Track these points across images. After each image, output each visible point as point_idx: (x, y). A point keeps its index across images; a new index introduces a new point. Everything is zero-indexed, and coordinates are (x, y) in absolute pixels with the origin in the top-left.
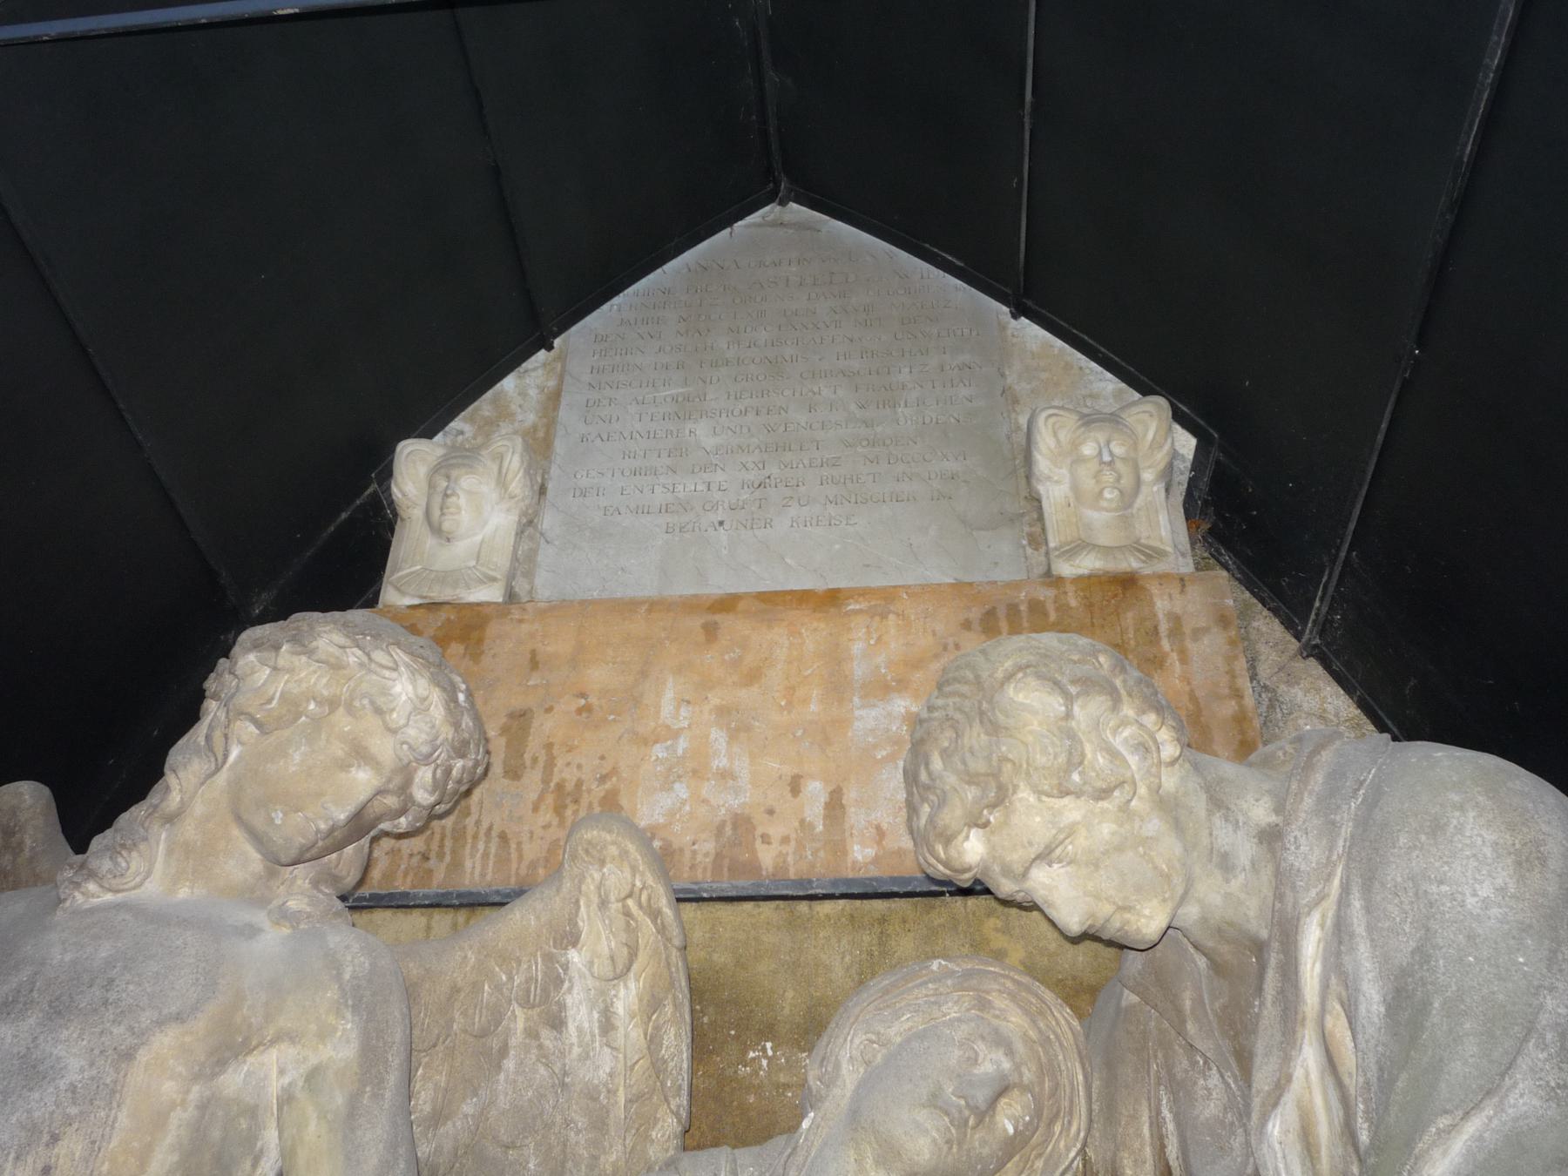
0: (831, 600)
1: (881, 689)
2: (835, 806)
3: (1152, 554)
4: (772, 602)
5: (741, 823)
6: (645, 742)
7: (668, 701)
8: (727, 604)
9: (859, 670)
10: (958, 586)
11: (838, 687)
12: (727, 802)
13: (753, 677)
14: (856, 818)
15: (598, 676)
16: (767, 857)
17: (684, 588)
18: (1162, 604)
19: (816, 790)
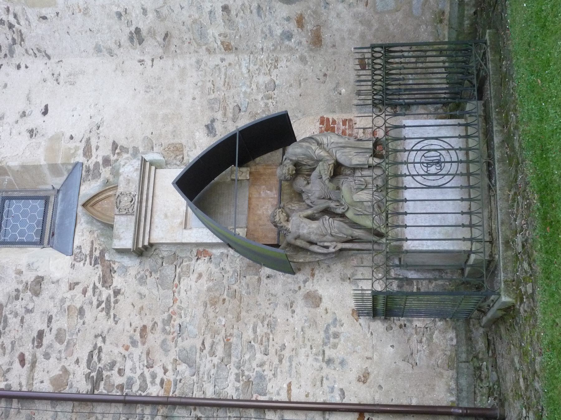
0: (250, 199)
1: (260, 194)
2: (271, 198)
3: (248, 170)
4: (249, 204)
5: (272, 206)
6: (264, 214)
7: (260, 212)
8: (249, 208)
9: (258, 196)
10: (250, 187)
11: (260, 198)
12: (270, 206)
13: (258, 205)
14: (273, 196)
15: (256, 219)
16: (276, 203)
17: (246, 212)
18: (253, 170)
19: (269, 200)
